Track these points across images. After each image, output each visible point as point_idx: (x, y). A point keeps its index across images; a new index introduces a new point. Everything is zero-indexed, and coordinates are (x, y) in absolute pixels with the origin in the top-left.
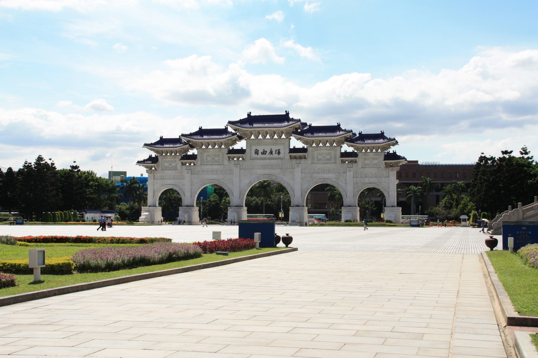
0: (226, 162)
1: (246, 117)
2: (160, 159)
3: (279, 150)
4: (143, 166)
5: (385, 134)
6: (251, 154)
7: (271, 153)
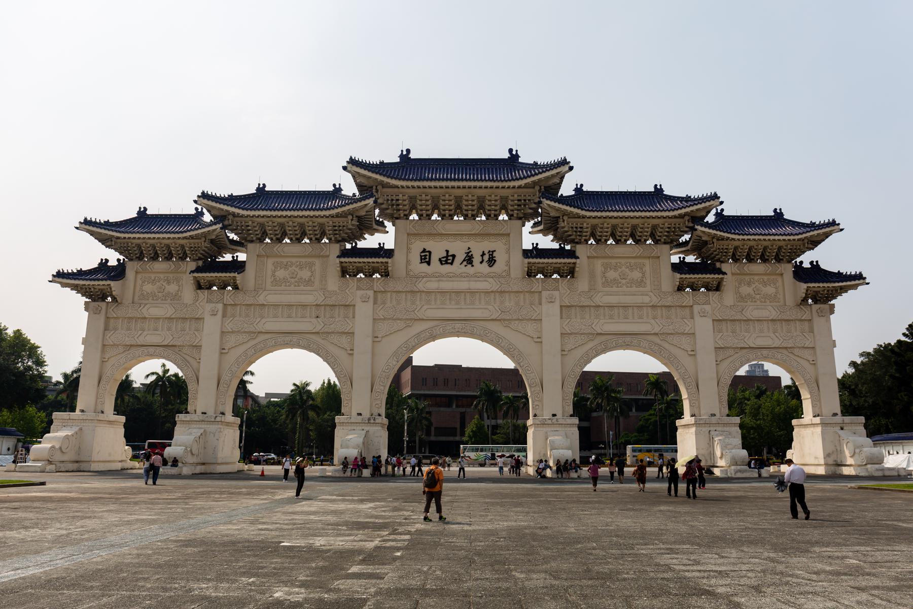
0: (334, 282)
1: (398, 160)
2: (130, 273)
3: (491, 253)
4: (75, 287)
6: (408, 262)
7: (469, 260)
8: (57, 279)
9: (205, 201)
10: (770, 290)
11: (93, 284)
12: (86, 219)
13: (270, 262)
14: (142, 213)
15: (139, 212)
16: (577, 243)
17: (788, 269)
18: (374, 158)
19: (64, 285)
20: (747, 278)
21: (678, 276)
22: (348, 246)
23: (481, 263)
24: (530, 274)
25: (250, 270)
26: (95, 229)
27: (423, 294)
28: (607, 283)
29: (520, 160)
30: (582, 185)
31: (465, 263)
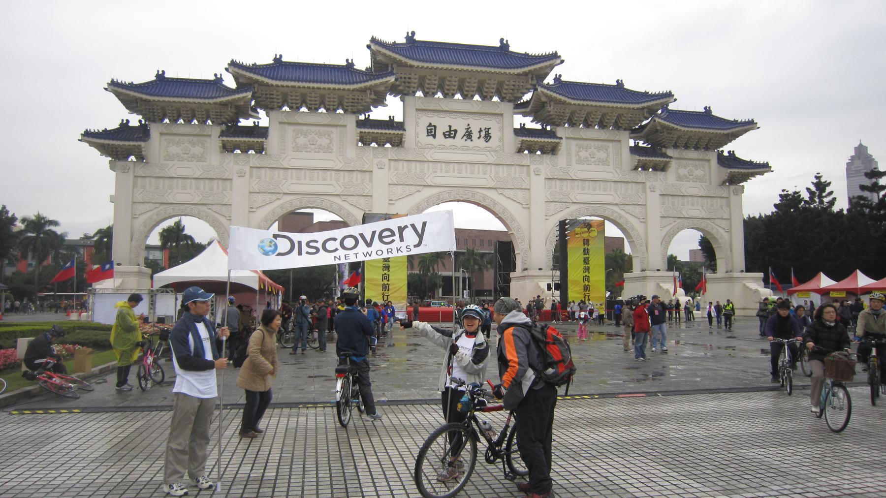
1: (404, 41)
3: (487, 130)
5: (714, 113)
6: (417, 134)
7: (469, 135)
8: (86, 138)
9: (236, 70)
10: (699, 172)
11: (117, 144)
12: (113, 80)
13: (291, 128)
14: (161, 77)
15: (158, 76)
16: (558, 125)
17: (713, 156)
18: (388, 39)
19: (91, 144)
20: (684, 162)
21: (638, 157)
22: (362, 117)
24: (520, 151)
25: (273, 135)
26: (120, 90)
27: (431, 164)
28: (580, 161)
29: (511, 49)
30: (560, 76)
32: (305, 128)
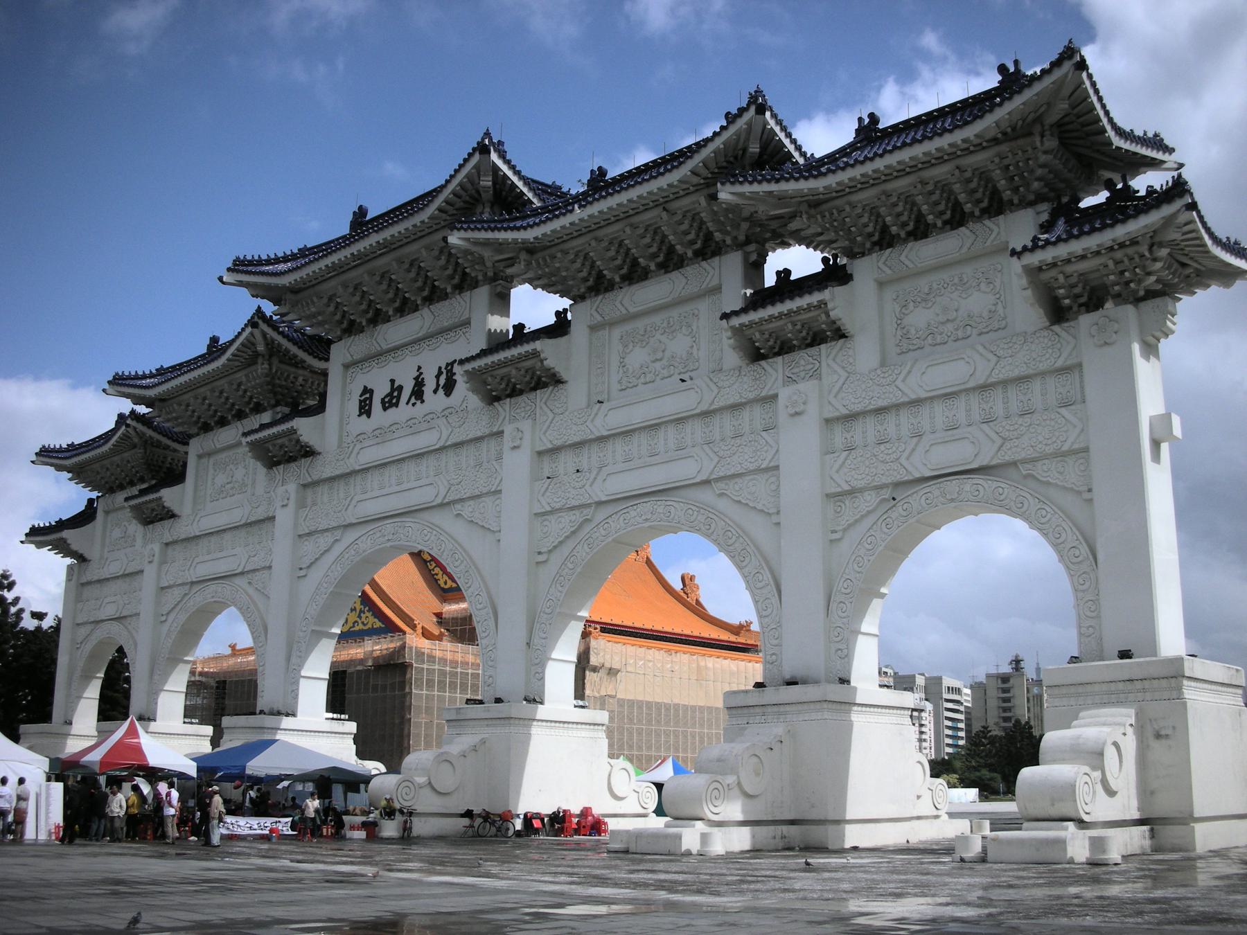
19: (40, 545)
23: (435, 391)
27: (359, 478)
31: (413, 400)
32: (223, 455)
